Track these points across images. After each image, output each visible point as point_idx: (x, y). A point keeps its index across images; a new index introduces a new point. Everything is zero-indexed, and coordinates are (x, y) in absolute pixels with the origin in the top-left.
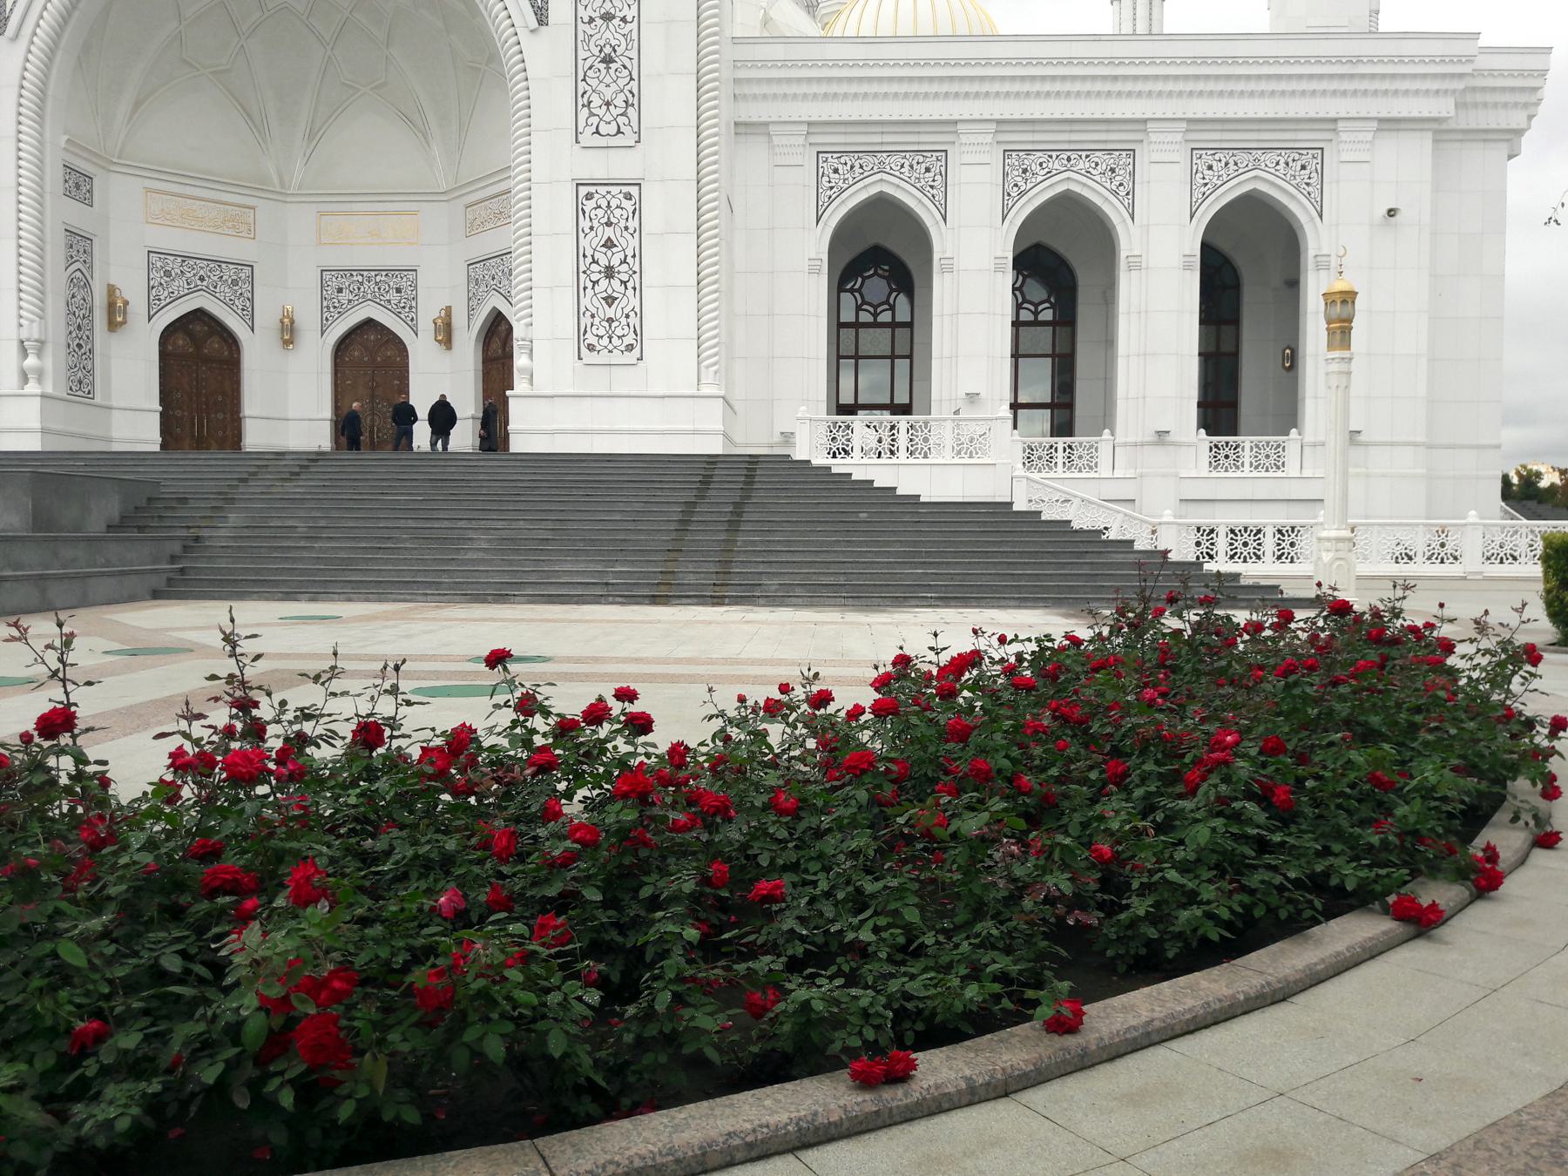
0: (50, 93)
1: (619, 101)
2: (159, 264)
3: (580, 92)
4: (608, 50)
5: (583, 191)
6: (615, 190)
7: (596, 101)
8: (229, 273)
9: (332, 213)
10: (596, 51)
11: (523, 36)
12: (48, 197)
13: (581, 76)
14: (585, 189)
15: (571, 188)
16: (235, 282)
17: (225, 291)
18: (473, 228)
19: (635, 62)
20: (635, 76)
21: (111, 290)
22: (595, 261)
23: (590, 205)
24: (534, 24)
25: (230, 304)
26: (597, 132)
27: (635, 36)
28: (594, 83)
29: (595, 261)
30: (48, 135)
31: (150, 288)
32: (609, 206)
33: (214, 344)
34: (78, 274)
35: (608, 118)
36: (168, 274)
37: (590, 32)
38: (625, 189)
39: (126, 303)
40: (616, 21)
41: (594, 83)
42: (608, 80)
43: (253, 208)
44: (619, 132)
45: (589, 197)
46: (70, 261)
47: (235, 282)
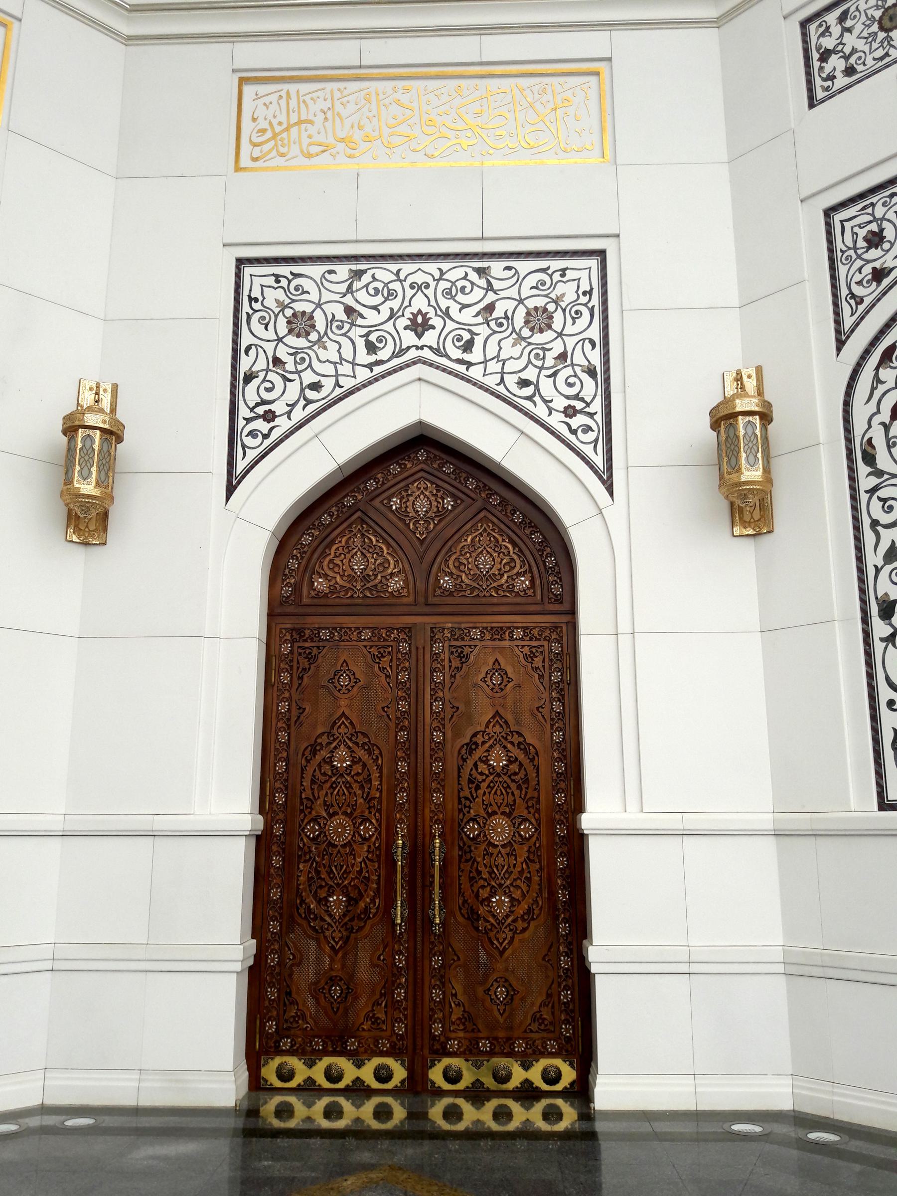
2: (272, 297)
16: (540, 320)
17: (503, 353)
25: (519, 397)
31: (239, 380)
33: (485, 558)
47: (540, 320)
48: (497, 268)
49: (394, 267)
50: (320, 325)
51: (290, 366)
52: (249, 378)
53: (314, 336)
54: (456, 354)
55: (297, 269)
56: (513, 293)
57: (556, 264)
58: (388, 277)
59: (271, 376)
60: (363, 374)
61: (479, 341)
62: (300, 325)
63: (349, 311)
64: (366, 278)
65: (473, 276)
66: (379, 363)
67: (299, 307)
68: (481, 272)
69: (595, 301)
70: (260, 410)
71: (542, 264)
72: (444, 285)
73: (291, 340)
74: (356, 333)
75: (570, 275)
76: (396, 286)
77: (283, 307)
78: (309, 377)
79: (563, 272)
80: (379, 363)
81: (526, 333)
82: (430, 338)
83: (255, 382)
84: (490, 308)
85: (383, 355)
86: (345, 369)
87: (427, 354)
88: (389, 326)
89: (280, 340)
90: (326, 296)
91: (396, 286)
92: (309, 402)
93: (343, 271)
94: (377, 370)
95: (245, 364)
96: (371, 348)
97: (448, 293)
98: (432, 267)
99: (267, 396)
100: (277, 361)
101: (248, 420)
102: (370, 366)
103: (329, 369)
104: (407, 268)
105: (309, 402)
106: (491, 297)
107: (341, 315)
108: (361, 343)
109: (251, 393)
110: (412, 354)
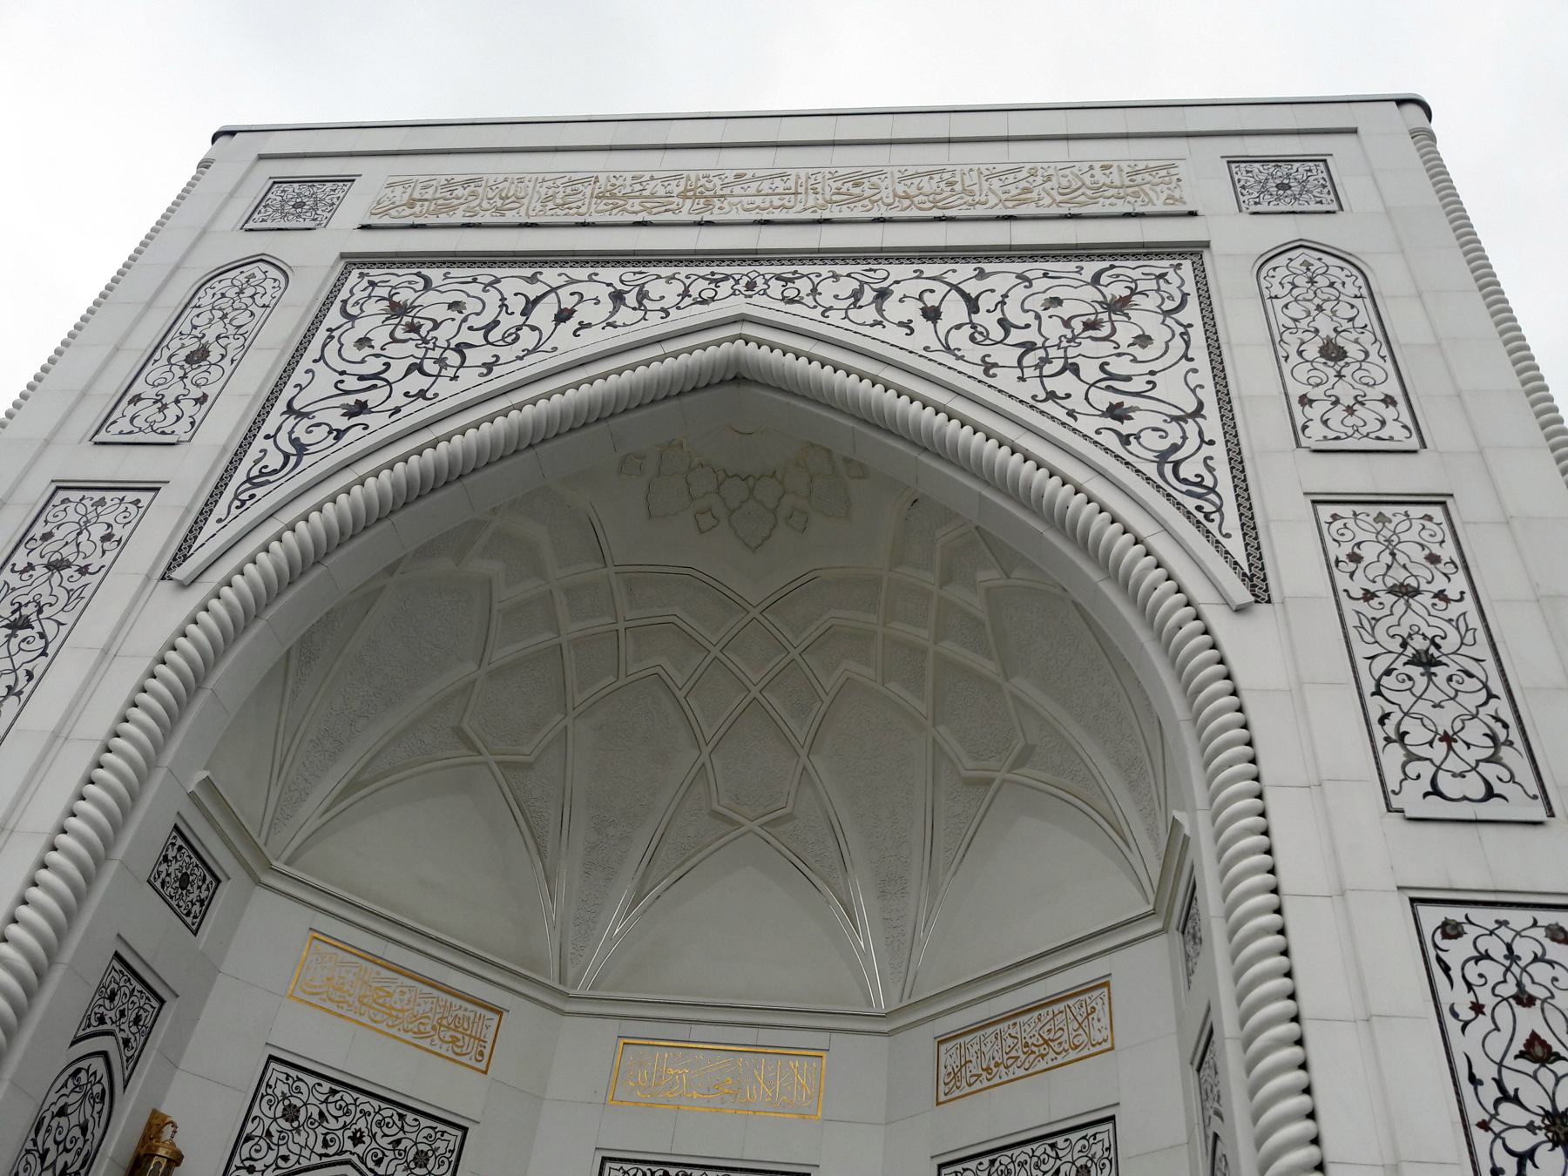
0: (211, 683)
1: (1474, 732)
2: (281, 1088)
3: (1375, 716)
4: (1419, 643)
5: (1432, 917)
6: (1520, 919)
7: (1417, 735)
8: (416, 1135)
9: (651, 1043)
10: (1395, 646)
11: (1218, 618)
12: (112, 868)
13: (1369, 686)
14: (1441, 914)
15: (1117, 1046)
18: (951, 1086)
19: (1490, 664)
20: (1497, 687)
21: (156, 1125)
22: (1506, 1097)
23: (1457, 951)
24: (1242, 594)
26: (1435, 791)
27: (1474, 620)
28: (1406, 700)
29: (1506, 1097)
30: (168, 757)
31: (243, 1138)
32: (1511, 955)
34: (98, 1065)
35: (1453, 764)
36: (291, 1113)
37: (1371, 613)
38: (1546, 918)
39: (176, 1159)
40: (1426, 599)
41: (1406, 700)
42: (1434, 695)
43: (499, 1012)
44: (1490, 794)
45: (1451, 930)
46: (94, 1026)
48: (410, 1117)
49: (355, 1095)
50: (302, 1118)
51: (275, 1140)
52: (248, 1138)
53: (295, 1124)
54: (371, 1164)
55: (301, 1075)
56: (413, 1136)
57: (441, 1127)
58: (349, 1099)
59: (262, 1142)
60: (315, 1160)
61: (386, 1160)
62: (290, 1113)
63: (321, 1114)
64: (338, 1097)
65: (396, 1118)
66: (327, 1155)
67: (295, 1101)
68: (401, 1117)
69: (453, 1158)
70: (247, 1163)
71: (434, 1124)
72: (378, 1117)
73: (282, 1122)
74: (320, 1130)
75: (446, 1136)
76: (352, 1108)
77: (285, 1097)
78: (283, 1151)
79: (443, 1133)
80: (327, 1155)
81: (412, 1165)
82: (360, 1149)
83: (251, 1143)
84: (398, 1142)
85: (331, 1151)
86: (306, 1153)
87: (355, 1159)
88: (339, 1133)
89: (275, 1119)
90: (312, 1100)
91: (352, 1108)
92: (278, 1168)
93: (326, 1086)
94: (325, 1160)
95: (250, 1128)
96: (326, 1144)
97: (379, 1124)
98: (376, 1103)
99: (255, 1155)
100: (269, 1134)
101: (238, 1168)
102: (321, 1156)
103: (296, 1149)
104: (363, 1098)
105: (278, 1168)
106: (401, 1135)
107: (316, 1116)
108: (321, 1138)
109: (245, 1149)
110: (346, 1156)
